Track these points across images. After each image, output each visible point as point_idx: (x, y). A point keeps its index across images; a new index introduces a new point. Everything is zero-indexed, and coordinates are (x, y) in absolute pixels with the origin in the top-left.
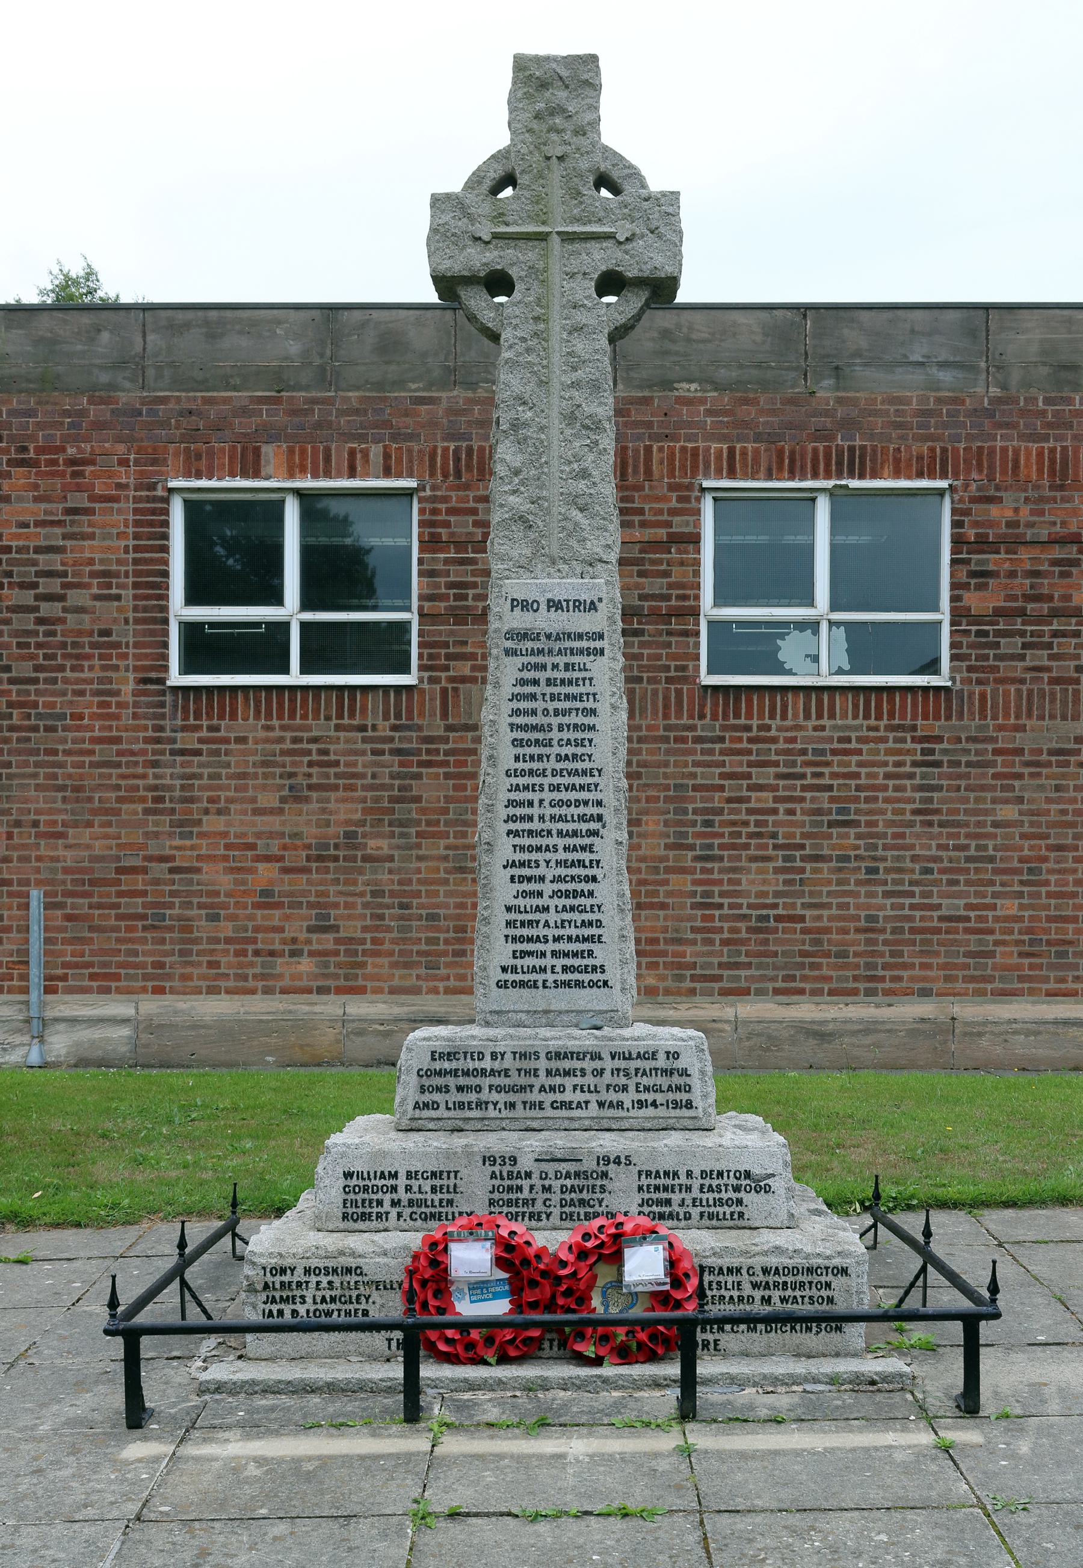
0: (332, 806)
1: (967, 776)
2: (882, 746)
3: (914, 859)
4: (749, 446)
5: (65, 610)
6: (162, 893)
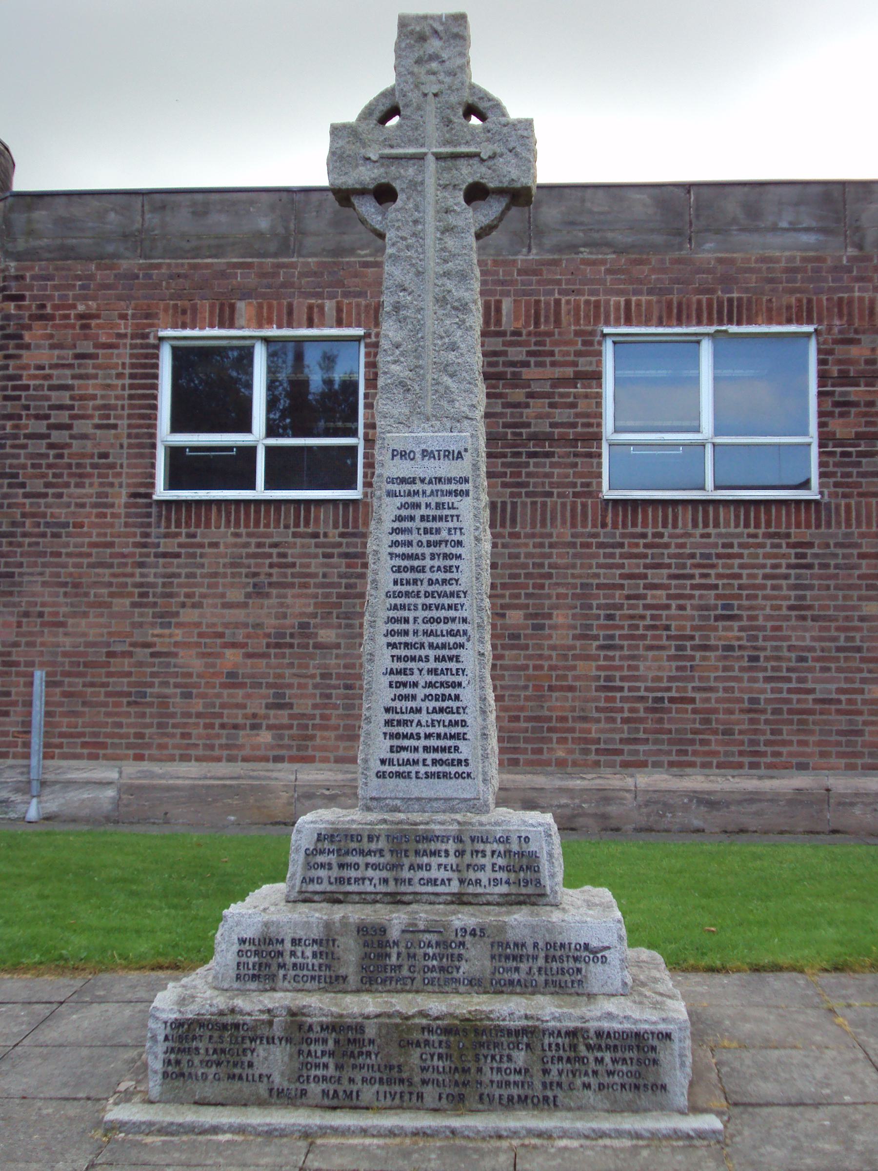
0: (289, 601)
1: (835, 577)
2: (760, 551)
3: (790, 648)
4: (644, 298)
5: (72, 437)
6: (144, 674)
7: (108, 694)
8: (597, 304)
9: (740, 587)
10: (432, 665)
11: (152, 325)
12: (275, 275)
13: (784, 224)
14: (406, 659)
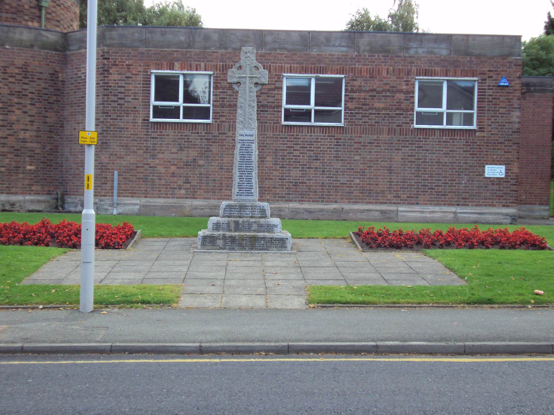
0: (190, 152)
1: (347, 148)
2: (326, 141)
3: (334, 168)
4: (295, 65)
5: (125, 102)
6: (147, 173)
7: (136, 178)
8: (282, 67)
9: (320, 151)
11: (149, 69)
12: (186, 54)
13: (337, 44)
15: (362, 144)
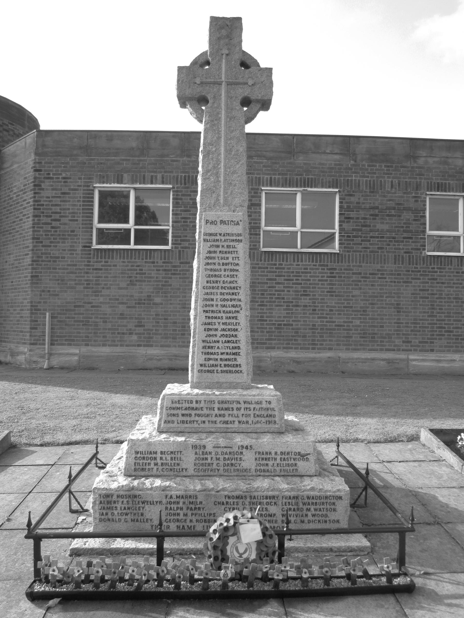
0: (143, 287)
1: (344, 281)
2: (317, 271)
3: (327, 306)
4: (277, 177)
8: (260, 178)
9: (310, 284)
10: (224, 321)
11: (91, 182)
13: (328, 151)
14: (212, 318)
15: (362, 275)
